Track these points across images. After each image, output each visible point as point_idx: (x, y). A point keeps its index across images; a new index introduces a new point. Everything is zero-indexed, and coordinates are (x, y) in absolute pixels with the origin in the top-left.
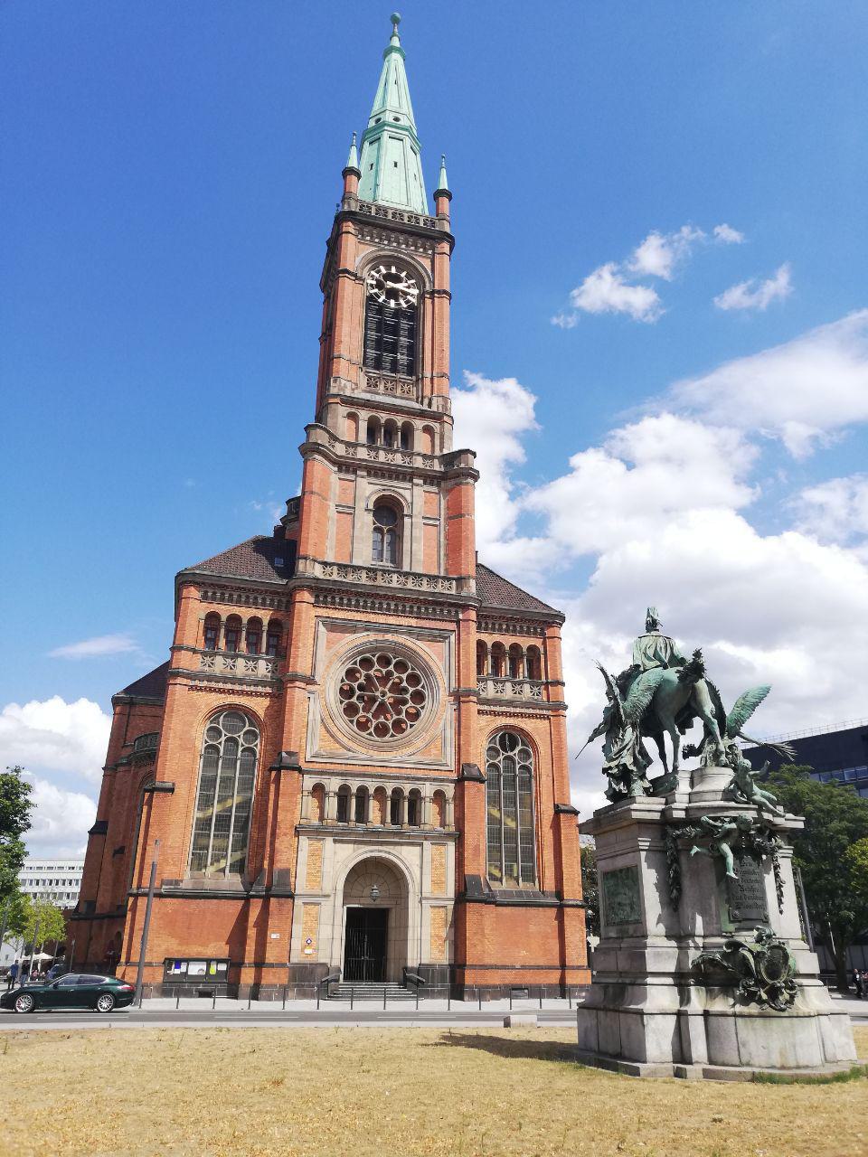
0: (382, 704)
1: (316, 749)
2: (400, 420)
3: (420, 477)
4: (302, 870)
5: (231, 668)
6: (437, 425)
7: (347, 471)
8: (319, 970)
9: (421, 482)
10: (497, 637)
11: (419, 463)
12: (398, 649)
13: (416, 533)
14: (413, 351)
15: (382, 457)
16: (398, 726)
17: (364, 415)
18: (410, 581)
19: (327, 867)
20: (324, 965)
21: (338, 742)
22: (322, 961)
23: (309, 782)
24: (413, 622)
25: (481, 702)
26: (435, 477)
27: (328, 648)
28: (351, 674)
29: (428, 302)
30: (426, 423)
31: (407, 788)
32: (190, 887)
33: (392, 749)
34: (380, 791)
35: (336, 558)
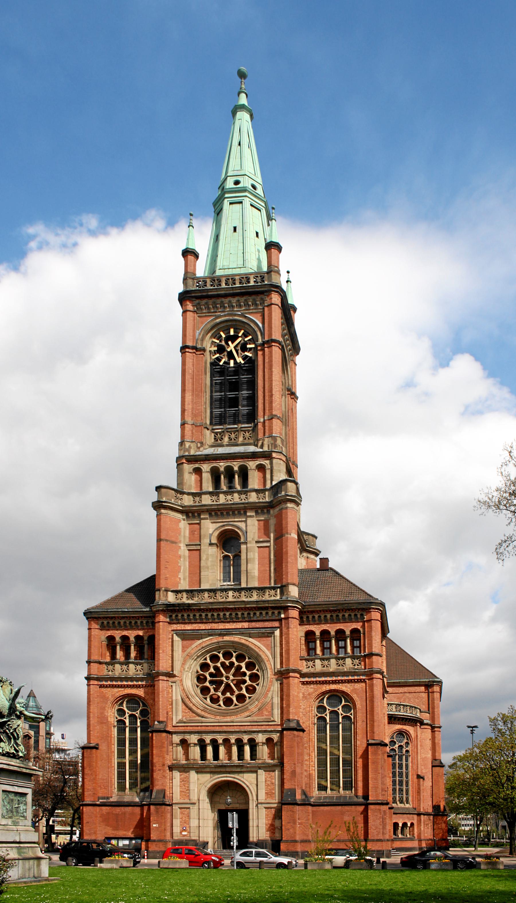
0: (228, 686)
1: (180, 717)
2: (236, 466)
3: (251, 509)
5: (126, 671)
6: (268, 462)
7: (194, 516)
9: (252, 513)
11: (253, 498)
12: (236, 645)
13: (251, 555)
14: (252, 400)
15: (222, 499)
16: (241, 698)
20: (194, 841)
21: (193, 712)
22: (193, 838)
23: (176, 739)
24: (246, 625)
25: (303, 675)
26: (264, 507)
28: (204, 667)
29: (260, 353)
30: (258, 462)
33: (235, 714)
35: (189, 585)
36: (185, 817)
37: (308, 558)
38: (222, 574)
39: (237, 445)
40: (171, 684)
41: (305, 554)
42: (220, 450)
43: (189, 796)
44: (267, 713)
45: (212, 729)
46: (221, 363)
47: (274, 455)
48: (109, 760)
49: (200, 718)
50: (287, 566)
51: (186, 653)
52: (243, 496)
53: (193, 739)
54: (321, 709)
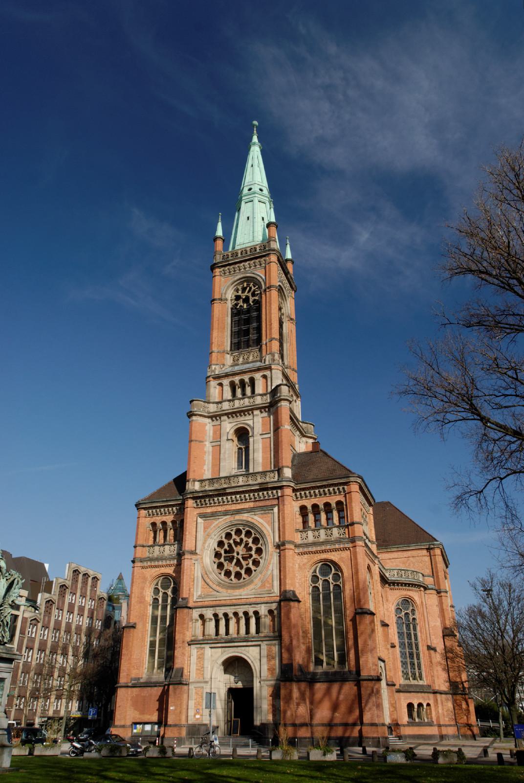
1: (199, 593)
2: (246, 378)
3: (257, 409)
4: (193, 668)
8: (203, 728)
10: (314, 501)
11: (259, 400)
14: (259, 329)
15: (237, 404)
17: (226, 382)
18: (250, 478)
19: (207, 664)
20: (206, 725)
23: (196, 614)
27: (205, 531)
28: (221, 544)
29: (263, 296)
37: (307, 442)
38: (236, 464)
39: (248, 363)
40: (193, 562)
41: (304, 439)
42: (237, 368)
43: (203, 674)
44: (268, 585)
45: (223, 602)
46: (238, 307)
47: (273, 367)
48: (143, 639)
49: (215, 593)
50: (282, 452)
51: (206, 533)
52: (252, 400)
53: (209, 613)
54: (315, 578)
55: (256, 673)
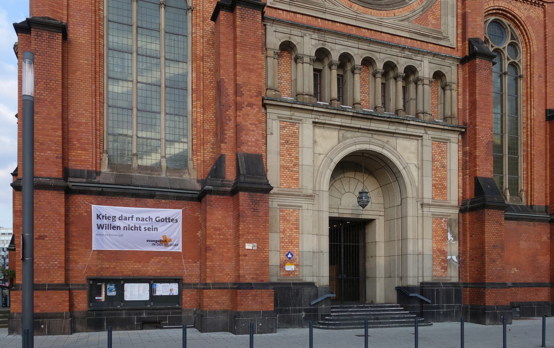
31: (402, 64)
32: (112, 181)
34: (368, 62)
36: (291, 230)
43: (297, 179)
44: (434, 21)
55: (410, 192)
